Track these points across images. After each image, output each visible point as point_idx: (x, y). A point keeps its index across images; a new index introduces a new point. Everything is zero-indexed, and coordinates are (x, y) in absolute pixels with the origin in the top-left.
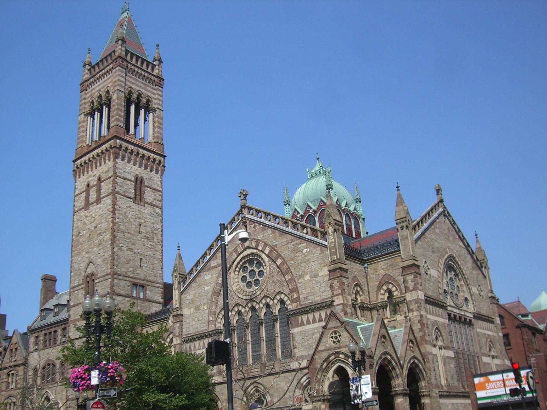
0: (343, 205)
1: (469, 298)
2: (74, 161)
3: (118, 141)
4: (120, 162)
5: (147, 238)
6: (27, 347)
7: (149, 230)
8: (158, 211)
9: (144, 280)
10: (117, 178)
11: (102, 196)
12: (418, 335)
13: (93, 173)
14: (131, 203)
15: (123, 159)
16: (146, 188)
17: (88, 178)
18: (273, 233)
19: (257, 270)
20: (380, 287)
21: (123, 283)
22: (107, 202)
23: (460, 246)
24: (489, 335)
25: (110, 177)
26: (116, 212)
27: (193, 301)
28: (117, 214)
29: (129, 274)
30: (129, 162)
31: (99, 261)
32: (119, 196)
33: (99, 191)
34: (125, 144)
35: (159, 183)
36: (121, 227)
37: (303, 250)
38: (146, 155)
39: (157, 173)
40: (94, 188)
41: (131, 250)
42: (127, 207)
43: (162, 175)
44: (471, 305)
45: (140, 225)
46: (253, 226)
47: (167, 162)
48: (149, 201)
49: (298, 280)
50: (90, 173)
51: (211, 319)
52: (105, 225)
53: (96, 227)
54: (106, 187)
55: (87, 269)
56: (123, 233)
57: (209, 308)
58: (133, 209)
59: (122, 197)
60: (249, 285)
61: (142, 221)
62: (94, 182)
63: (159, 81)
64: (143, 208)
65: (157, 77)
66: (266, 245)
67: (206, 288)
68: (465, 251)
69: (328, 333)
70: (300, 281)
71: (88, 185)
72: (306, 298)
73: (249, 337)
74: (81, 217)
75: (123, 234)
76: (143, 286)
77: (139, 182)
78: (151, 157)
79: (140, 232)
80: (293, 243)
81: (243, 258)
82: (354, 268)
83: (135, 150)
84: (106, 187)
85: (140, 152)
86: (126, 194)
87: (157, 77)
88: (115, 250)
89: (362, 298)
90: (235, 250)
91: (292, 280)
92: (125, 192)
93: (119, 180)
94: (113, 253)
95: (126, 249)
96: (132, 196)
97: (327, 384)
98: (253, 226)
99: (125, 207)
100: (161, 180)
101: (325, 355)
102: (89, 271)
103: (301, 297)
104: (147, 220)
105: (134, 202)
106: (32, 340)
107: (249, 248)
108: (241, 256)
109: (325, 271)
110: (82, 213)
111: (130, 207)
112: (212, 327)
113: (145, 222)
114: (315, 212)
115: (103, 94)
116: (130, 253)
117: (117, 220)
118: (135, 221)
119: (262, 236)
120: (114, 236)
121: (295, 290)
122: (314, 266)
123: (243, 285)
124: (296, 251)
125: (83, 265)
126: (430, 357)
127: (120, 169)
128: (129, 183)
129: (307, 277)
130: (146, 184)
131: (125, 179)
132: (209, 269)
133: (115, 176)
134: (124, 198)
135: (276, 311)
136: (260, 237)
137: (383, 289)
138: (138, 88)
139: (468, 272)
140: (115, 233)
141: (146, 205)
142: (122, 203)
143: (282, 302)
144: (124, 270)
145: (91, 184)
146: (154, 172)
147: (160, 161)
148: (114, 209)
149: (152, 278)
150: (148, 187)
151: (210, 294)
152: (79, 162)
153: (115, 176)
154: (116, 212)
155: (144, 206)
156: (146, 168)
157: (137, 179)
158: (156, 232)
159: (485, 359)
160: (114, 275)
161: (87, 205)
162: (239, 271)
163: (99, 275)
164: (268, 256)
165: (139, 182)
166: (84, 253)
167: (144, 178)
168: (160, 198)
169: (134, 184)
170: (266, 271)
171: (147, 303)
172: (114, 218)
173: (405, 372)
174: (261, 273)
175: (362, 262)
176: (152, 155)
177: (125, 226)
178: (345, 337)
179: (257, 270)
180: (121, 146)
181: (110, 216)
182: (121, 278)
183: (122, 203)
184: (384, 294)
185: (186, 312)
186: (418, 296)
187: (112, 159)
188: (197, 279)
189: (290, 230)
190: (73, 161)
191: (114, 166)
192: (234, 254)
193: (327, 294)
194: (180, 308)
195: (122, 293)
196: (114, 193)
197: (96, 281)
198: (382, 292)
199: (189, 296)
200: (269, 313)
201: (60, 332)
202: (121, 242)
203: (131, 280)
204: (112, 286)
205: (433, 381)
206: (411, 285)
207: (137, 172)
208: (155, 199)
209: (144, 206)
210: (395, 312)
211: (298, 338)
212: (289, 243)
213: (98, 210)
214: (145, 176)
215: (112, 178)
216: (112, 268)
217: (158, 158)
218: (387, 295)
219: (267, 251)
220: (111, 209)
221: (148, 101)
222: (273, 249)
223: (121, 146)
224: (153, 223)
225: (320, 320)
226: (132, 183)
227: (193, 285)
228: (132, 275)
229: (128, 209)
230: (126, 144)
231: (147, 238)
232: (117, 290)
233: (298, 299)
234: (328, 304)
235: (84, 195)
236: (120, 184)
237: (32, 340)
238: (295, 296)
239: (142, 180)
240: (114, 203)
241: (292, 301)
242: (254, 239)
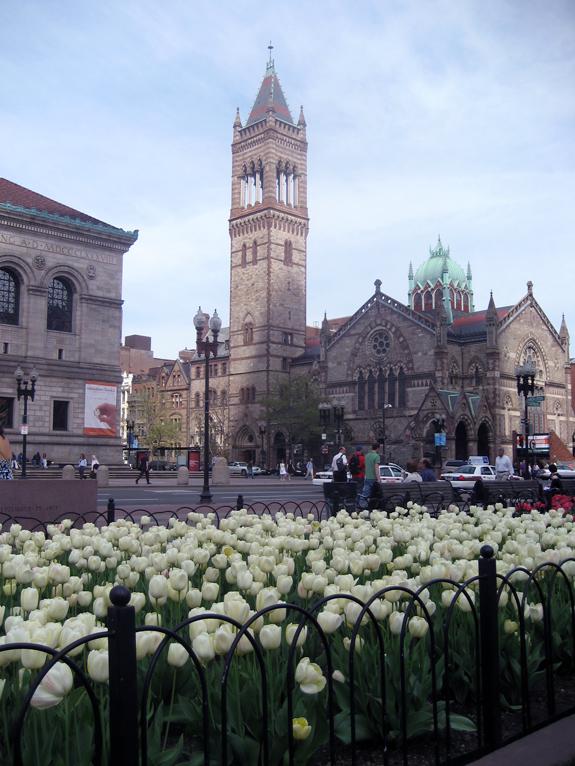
0: (455, 285)
1: (544, 370)
2: (230, 221)
6: (188, 376)
8: (303, 269)
9: (292, 329)
12: (491, 401)
14: (282, 265)
18: (398, 317)
19: (385, 342)
20: (470, 364)
21: (276, 333)
22: (264, 264)
23: (543, 329)
24: (558, 399)
27: (335, 358)
29: (281, 325)
33: (255, 253)
34: (277, 213)
36: (276, 287)
43: (306, 236)
44: (544, 376)
47: (311, 224)
50: (246, 235)
51: (349, 372)
57: (348, 365)
60: (378, 352)
62: (250, 244)
63: (303, 145)
65: (302, 142)
66: (393, 325)
67: (347, 350)
68: (547, 333)
69: (429, 399)
71: (244, 245)
72: (418, 369)
73: (376, 389)
76: (291, 334)
77: (288, 245)
79: (289, 290)
82: (454, 350)
84: (261, 251)
87: (302, 142)
90: (370, 325)
91: (409, 354)
93: (273, 246)
97: (425, 430)
101: (426, 412)
102: (249, 319)
106: (193, 370)
107: (380, 325)
109: (432, 352)
110: (239, 269)
111: (281, 269)
112: (350, 379)
114: (432, 290)
115: (256, 162)
116: (281, 308)
121: (411, 361)
122: (425, 348)
123: (374, 351)
124: (413, 334)
125: (242, 315)
126: (498, 417)
129: (420, 354)
132: (350, 335)
133: (269, 242)
135: (397, 373)
136: (388, 318)
138: (286, 157)
139: (546, 350)
143: (401, 368)
144: (277, 322)
145: (247, 245)
149: (297, 327)
151: (349, 355)
152: (234, 222)
157: (286, 243)
159: (549, 417)
161: (244, 263)
164: (394, 333)
165: (288, 245)
170: (392, 344)
171: (293, 348)
173: (477, 427)
174: (388, 345)
175: (460, 345)
178: (438, 404)
179: (385, 342)
183: (276, 266)
185: (330, 365)
188: (340, 342)
189: (410, 317)
193: (432, 368)
194: (325, 362)
195: (277, 341)
199: (333, 353)
200: (391, 374)
201: (220, 366)
204: (268, 336)
205: (498, 433)
206: (491, 366)
210: (479, 382)
211: (411, 395)
214: (292, 240)
217: (303, 221)
219: (393, 330)
221: (294, 167)
222: (397, 329)
225: (426, 385)
227: (337, 346)
232: (272, 339)
233: (412, 368)
234: (431, 375)
235: (240, 254)
237: (193, 370)
241: (408, 369)
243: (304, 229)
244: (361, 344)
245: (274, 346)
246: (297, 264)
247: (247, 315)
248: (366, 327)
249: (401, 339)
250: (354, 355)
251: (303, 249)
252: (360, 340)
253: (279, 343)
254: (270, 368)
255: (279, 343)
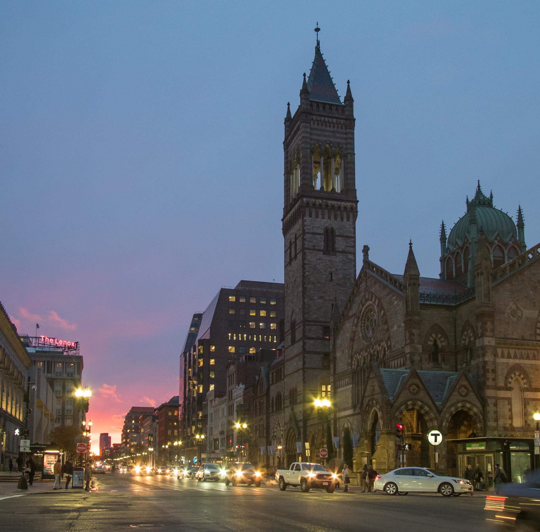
3: (305, 199)
4: (309, 219)
5: (339, 284)
7: (341, 276)
10: (306, 235)
11: (297, 252)
13: (293, 231)
14: (321, 255)
15: (310, 216)
16: (337, 238)
17: (290, 236)
22: (300, 256)
25: (300, 236)
26: (305, 266)
28: (307, 268)
29: (321, 319)
30: (317, 217)
31: (297, 310)
32: (308, 251)
35: (352, 230)
36: (312, 279)
37: (394, 302)
38: (335, 205)
39: (348, 220)
40: (294, 245)
41: (321, 298)
42: (317, 259)
45: (331, 274)
46: (370, 279)
47: (360, 207)
48: (340, 250)
49: (391, 330)
50: (291, 231)
52: (300, 279)
53: (295, 280)
54: (299, 244)
55: (292, 317)
56: (313, 283)
58: (324, 260)
59: (312, 251)
61: (334, 270)
64: (333, 257)
66: (376, 297)
70: (392, 330)
71: (291, 242)
72: (394, 346)
74: (288, 271)
75: (313, 286)
78: (341, 206)
79: (331, 280)
80: (390, 296)
81: (366, 308)
83: (323, 204)
84: (299, 244)
85: (329, 204)
86: (315, 248)
88: (305, 300)
89: (444, 344)
92: (314, 246)
93: (307, 236)
94: (304, 303)
95: (316, 298)
96: (322, 248)
98: (370, 279)
99: (315, 260)
100: (354, 226)
102: (293, 320)
103: (393, 344)
104: (338, 268)
105: (324, 254)
108: (365, 307)
110: (289, 268)
111: (319, 259)
113: (337, 270)
116: (320, 301)
117: (307, 273)
118: (325, 271)
119: (374, 289)
120: (304, 288)
127: (308, 226)
128: (318, 236)
129: (395, 328)
130: (337, 234)
131: (314, 234)
134: (314, 252)
136: (373, 290)
137: (464, 335)
140: (306, 286)
141: (338, 254)
142: (311, 257)
144: (314, 316)
146: (345, 219)
147: (352, 208)
148: (304, 264)
150: (339, 236)
152: (285, 220)
153: (304, 233)
154: (305, 266)
155: (336, 255)
156: (336, 218)
157: (327, 230)
158: (349, 277)
160: (305, 322)
162: (365, 320)
163: (297, 322)
166: (290, 303)
167: (335, 228)
168: (353, 245)
169: (323, 236)
172: (304, 273)
176: (343, 203)
177: (316, 277)
180: (308, 203)
181: (301, 271)
182: (312, 323)
183: (311, 257)
184: (465, 340)
186: (483, 343)
187: (301, 218)
190: (282, 220)
191: (303, 225)
192: (361, 305)
196: (303, 249)
197: (296, 327)
198: (464, 337)
202: (311, 292)
203: (323, 324)
207: (327, 225)
208: (347, 246)
209: (336, 255)
212: (388, 295)
213: (295, 265)
215: (302, 235)
216: (303, 316)
218: (467, 340)
220: (302, 265)
223: (308, 203)
224: (345, 269)
226: (322, 236)
228: (323, 320)
229: (319, 261)
230: (313, 200)
231: (339, 284)
236: (309, 240)
238: (389, 344)
239: (333, 231)
240: (304, 258)
242: (370, 292)
243: (353, 213)
244: (356, 326)
245: (312, 342)
246: (343, 252)
247: (292, 314)
248: (359, 305)
249: (382, 312)
250: (352, 340)
251: (352, 235)
252: (356, 322)
253: (318, 339)
254: (306, 366)
255: (318, 339)
